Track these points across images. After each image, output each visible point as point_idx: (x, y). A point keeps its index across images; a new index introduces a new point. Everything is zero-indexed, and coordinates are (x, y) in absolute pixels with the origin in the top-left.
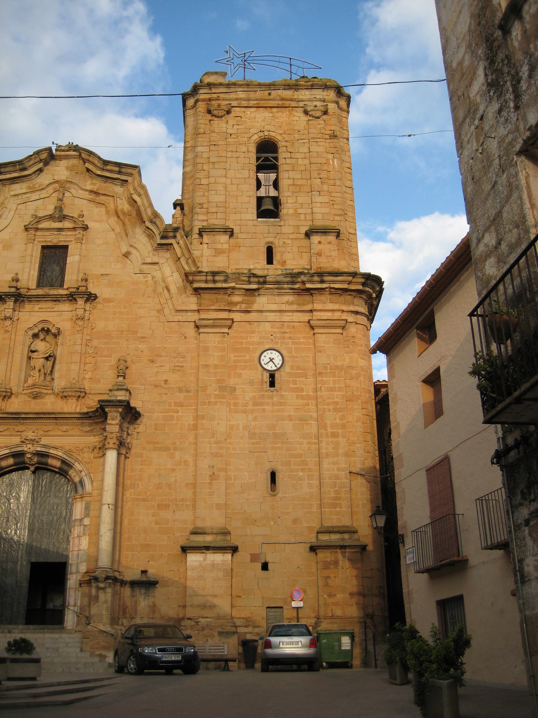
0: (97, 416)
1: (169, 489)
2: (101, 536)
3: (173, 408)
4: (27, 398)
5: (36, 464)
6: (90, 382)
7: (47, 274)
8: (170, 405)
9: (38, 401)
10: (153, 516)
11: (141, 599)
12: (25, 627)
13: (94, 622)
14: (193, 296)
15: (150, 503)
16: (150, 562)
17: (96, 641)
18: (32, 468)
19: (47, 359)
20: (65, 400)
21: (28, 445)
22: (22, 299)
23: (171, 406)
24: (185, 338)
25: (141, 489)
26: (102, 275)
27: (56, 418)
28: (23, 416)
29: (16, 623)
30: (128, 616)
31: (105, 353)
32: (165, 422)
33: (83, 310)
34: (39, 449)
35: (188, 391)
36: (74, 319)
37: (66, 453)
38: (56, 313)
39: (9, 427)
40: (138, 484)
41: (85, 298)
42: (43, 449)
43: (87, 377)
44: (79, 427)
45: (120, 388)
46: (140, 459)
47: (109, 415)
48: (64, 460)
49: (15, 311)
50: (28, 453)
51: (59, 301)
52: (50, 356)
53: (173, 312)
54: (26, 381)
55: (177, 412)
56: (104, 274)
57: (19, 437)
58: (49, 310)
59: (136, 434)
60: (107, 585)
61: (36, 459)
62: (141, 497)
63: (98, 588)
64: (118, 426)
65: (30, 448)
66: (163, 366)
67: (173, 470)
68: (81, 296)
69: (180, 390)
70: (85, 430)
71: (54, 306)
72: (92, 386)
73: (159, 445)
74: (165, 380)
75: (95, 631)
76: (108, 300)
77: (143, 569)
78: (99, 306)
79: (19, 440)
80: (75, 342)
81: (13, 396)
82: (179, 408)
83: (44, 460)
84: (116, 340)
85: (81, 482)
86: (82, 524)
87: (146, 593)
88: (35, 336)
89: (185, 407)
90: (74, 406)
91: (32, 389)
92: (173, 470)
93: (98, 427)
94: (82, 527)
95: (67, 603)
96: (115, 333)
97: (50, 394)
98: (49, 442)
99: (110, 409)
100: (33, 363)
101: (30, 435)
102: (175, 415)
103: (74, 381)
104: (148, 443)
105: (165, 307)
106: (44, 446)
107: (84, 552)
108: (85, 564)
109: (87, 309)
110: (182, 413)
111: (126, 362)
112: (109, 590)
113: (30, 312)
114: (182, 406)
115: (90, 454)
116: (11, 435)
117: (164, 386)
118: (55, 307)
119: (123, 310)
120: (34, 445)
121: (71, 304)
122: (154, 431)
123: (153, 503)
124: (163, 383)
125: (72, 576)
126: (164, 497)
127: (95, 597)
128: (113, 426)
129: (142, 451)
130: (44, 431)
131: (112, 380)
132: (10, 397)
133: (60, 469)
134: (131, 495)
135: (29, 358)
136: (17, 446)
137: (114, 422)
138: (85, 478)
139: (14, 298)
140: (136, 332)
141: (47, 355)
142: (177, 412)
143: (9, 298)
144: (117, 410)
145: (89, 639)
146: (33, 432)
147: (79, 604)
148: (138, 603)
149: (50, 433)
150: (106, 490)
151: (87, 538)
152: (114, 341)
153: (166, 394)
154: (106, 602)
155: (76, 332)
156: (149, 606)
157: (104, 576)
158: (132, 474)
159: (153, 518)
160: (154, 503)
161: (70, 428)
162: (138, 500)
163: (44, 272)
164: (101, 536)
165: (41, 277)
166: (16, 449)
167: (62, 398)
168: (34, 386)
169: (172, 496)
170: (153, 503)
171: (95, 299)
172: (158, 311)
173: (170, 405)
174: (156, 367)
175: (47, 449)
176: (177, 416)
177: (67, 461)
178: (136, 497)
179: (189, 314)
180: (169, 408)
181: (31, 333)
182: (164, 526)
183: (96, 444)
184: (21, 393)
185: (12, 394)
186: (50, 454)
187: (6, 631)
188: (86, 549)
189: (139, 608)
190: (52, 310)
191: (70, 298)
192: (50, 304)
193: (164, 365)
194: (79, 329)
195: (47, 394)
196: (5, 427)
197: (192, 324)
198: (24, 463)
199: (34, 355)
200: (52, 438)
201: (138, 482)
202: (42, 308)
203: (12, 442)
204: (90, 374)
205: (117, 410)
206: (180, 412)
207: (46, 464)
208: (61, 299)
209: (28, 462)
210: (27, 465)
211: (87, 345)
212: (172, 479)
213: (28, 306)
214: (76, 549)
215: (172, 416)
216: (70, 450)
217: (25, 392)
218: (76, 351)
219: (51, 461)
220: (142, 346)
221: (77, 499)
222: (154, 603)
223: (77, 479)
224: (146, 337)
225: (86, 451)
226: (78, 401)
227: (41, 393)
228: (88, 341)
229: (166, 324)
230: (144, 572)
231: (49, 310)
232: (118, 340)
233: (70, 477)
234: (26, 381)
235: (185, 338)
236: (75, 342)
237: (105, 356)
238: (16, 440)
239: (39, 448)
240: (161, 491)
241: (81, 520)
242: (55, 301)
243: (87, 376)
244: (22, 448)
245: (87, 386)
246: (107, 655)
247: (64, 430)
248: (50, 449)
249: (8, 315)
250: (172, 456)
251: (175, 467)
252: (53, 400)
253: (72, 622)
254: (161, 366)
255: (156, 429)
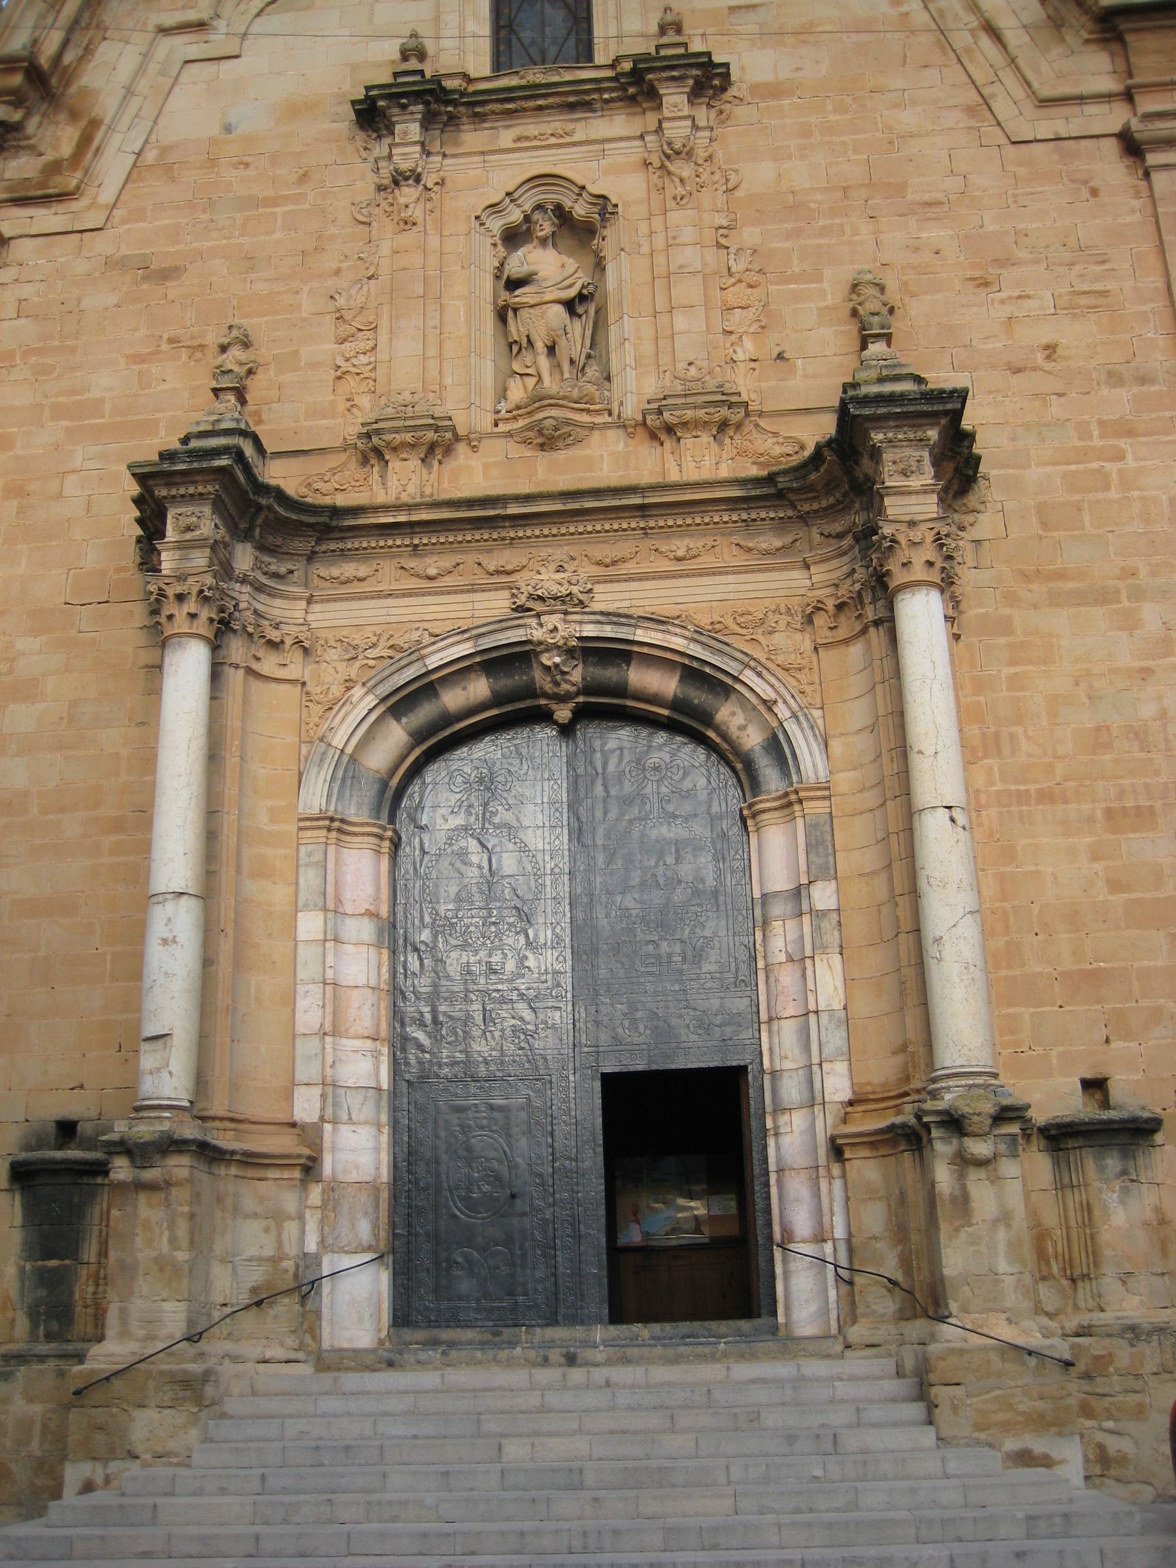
0: (811, 488)
1: (1142, 750)
2: (938, 940)
3: (1097, 442)
4: (515, 450)
5: (578, 694)
6: (756, 373)
7: (522, 35)
8: (1085, 435)
9: (562, 455)
10: (1095, 857)
11: (1112, 1198)
12: (614, 1331)
13: (966, 1311)
14: (1093, 47)
15: (1072, 806)
16: (1113, 1045)
17: (998, 1392)
18: (563, 714)
19: (570, 306)
20: (668, 445)
21: (544, 618)
22: (450, 109)
23: (1091, 437)
24: (1094, 192)
25: (1029, 756)
26: (732, 9)
27: (642, 510)
28: (513, 509)
29: (574, 1320)
30: (1055, 1268)
31: (796, 266)
32: (1077, 497)
33: (689, 123)
34: (590, 631)
35: (1143, 380)
36: (655, 160)
37: (703, 639)
38: (585, 148)
39: (458, 558)
40: (1012, 736)
41: (691, 82)
42: (608, 628)
43: (740, 356)
44: (736, 539)
45: (885, 373)
46: (1002, 641)
47: (887, 456)
48: (695, 665)
49: (429, 154)
50: (549, 648)
51: (587, 106)
52: (582, 298)
53: (1028, 108)
54: (503, 394)
55: (1120, 456)
56: (740, 7)
57: (506, 594)
58: (553, 141)
59: (969, 547)
60: (1002, 1148)
61: (576, 675)
62: (1032, 787)
63: (964, 1162)
64: (934, 498)
65: (556, 629)
66: (1029, 297)
67: (1145, 673)
68: (675, 73)
69: (1114, 378)
70: (764, 546)
71: (569, 127)
72: (764, 385)
73: (1070, 585)
74: (1047, 347)
75: (985, 1349)
76: (773, 91)
77: (1088, 1075)
78: (741, 112)
79: (507, 604)
80: (674, 238)
81: (461, 448)
82: (1123, 443)
83: (610, 674)
84: (829, 222)
85: (777, 747)
86: (805, 907)
87: (1124, 1172)
88: (513, 237)
89: (1144, 435)
90: (708, 462)
91: (529, 413)
92: (1145, 673)
93: (815, 531)
94: (806, 919)
95: (777, 1229)
96: (819, 197)
97: (605, 426)
98: (627, 604)
99: (890, 435)
100: (516, 329)
101: (550, 581)
102: (1111, 467)
103: (693, 371)
104: (1026, 577)
105: (993, 96)
106: (610, 617)
107: (831, 1017)
108: (841, 1067)
109: (702, 123)
110: (1136, 459)
111: (882, 289)
112: (1009, 1168)
113: (483, 153)
114: (1130, 433)
115: (799, 636)
116: (473, 589)
117: (1049, 366)
118: (573, 131)
119: (833, 118)
120: (570, 617)
121: (634, 114)
122: (1041, 532)
123: (1086, 807)
124: (1040, 357)
125: (784, 1119)
126: (1126, 782)
127: (953, 1199)
128: (913, 499)
129: (1007, 611)
130: (598, 563)
131: (837, 358)
132: (448, 450)
133: (677, 705)
134: (991, 782)
135: (502, 315)
136: (502, 624)
137: (915, 483)
138: (791, 727)
139: (420, 107)
140: (901, 189)
141: (572, 293)
142: (1120, 456)
143: (404, 107)
144: (920, 434)
145: (962, 1387)
146: (560, 569)
147: (840, 1232)
148: (1097, 1212)
149: (630, 568)
150: (929, 751)
151: (836, 960)
152: (822, 222)
153: (1060, 395)
154: (1005, 1218)
155: (671, 204)
156: (1146, 1224)
157: (989, 1108)
158: (982, 699)
159: (1098, 866)
160: (1090, 806)
161: (700, 544)
162: (1022, 797)
163: (512, 29)
164: (938, 940)
165: (502, 47)
166: (499, 636)
167: (653, 436)
168: (538, 400)
169: (1157, 773)
170: (1086, 807)
171: (724, 89)
172: (970, 111)
173: (1085, 435)
174: (1002, 302)
175: (625, 629)
176: (1120, 471)
177: (707, 670)
178: (1013, 787)
179: (1091, 109)
180: (1081, 443)
181: (496, 225)
182: (1148, 895)
183: (820, 593)
184: (491, 435)
185: (457, 438)
186: (636, 649)
187: (555, 1355)
188: (837, 1005)
189: (1105, 1236)
190: (568, 140)
191: (631, 90)
192: (554, 123)
193: (1032, 293)
194: (680, 190)
195: (593, 427)
196: (447, 562)
197: (1111, 147)
198: (532, 692)
199: (525, 295)
200: (634, 585)
201: (1014, 729)
202: (527, 138)
203: (477, 614)
204: (748, 343)
205: (920, 434)
206: (1129, 457)
207: (621, 690)
208: (595, 96)
209: (548, 687)
210: (543, 702)
211: (719, 246)
212: (1148, 711)
213: (472, 138)
214: (791, 1011)
215: (1099, 471)
216: (718, 626)
217: (503, 427)
218: (681, 267)
219: (642, 678)
220: (935, 234)
221: (764, 816)
222: (1158, 1210)
223: (752, 739)
224: (941, 203)
225: (782, 624)
226: (721, 444)
227: (568, 422)
228: (725, 231)
229: (1010, 150)
230: (1095, 1086)
231: (553, 141)
232: (838, 221)
233: (724, 736)
234: (503, 394)
235: (1094, 192)
236: (674, 238)
237: (795, 279)
238: (497, 604)
239: (591, 627)
240: (1108, 757)
241: (798, 893)
242: (572, 107)
243: (739, 350)
244: (522, 631)
245: (745, 384)
246: (1055, 1454)
247: (680, 553)
248: (636, 626)
249: (405, 166)
250: (1130, 623)
251: (1149, 663)
252: (621, 447)
253: (813, 1308)
254: (1020, 297)
255: (1044, 525)
